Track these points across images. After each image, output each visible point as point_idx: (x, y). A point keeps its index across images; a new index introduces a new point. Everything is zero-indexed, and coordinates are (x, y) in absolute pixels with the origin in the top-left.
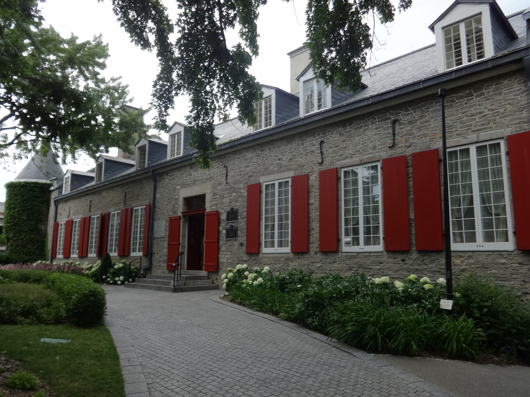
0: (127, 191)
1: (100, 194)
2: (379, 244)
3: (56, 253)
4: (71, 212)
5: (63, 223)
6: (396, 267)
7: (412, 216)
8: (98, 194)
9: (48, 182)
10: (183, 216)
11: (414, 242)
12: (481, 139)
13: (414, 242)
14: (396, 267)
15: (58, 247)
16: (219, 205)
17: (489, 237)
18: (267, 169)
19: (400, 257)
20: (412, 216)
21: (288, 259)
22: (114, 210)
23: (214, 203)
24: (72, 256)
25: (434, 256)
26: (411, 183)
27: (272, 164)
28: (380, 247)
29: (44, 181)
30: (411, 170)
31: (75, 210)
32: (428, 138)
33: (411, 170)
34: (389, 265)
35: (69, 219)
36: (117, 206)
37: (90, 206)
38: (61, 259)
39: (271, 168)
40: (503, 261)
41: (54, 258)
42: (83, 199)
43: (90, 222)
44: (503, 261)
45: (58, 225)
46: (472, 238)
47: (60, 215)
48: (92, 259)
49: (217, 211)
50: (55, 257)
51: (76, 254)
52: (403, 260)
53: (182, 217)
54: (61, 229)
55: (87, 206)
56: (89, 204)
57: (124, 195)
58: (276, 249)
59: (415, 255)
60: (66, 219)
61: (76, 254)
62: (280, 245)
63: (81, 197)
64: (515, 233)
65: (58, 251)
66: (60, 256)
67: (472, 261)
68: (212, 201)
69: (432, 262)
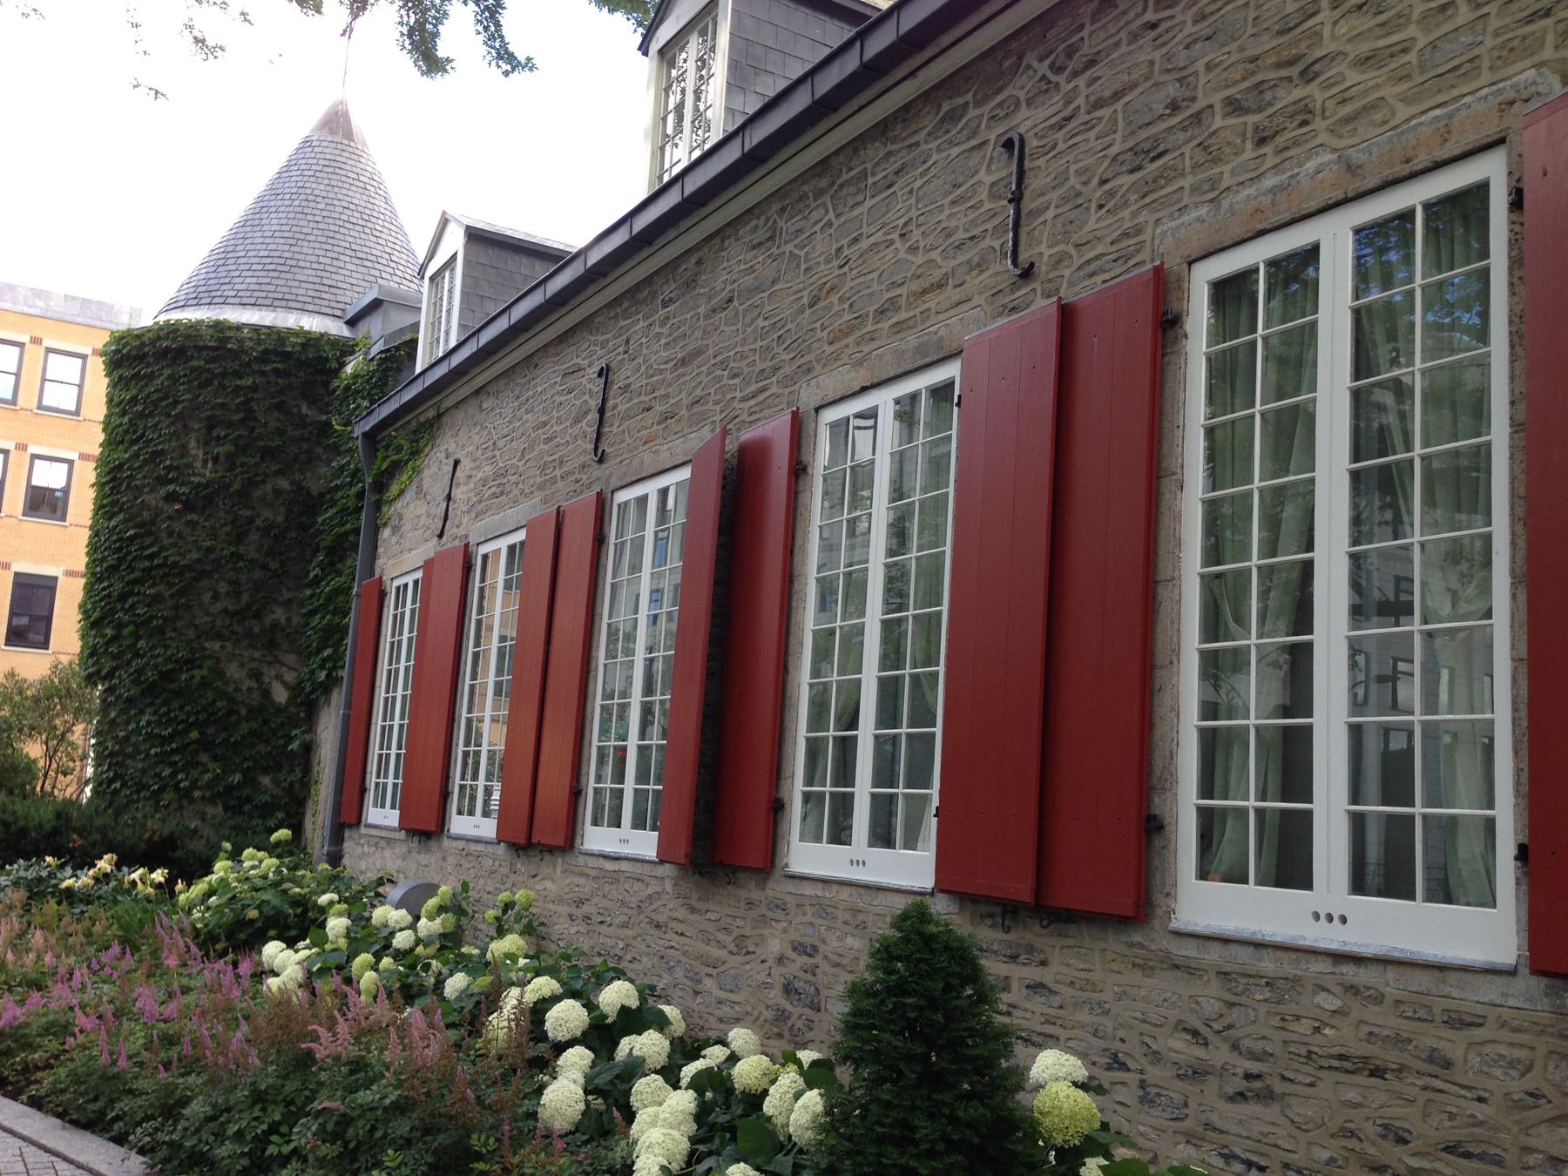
0: (1026, 121)
1: (691, 284)
3: (363, 790)
4: (458, 493)
5: (410, 579)
8: (667, 291)
9: (337, 329)
15: (375, 751)
22: (862, 377)
24: (460, 824)
29: (312, 324)
31: (488, 470)
35: (451, 542)
36: (899, 327)
37: (602, 411)
38: (383, 839)
41: (350, 826)
42: (547, 381)
43: (600, 540)
45: (382, 595)
47: (395, 529)
48: (615, 878)
50: (357, 821)
51: (486, 814)
54: (398, 620)
55: (577, 420)
56: (594, 403)
57: (994, 171)
60: (428, 550)
61: (486, 814)
63: (529, 362)
65: (372, 780)
66: (381, 815)
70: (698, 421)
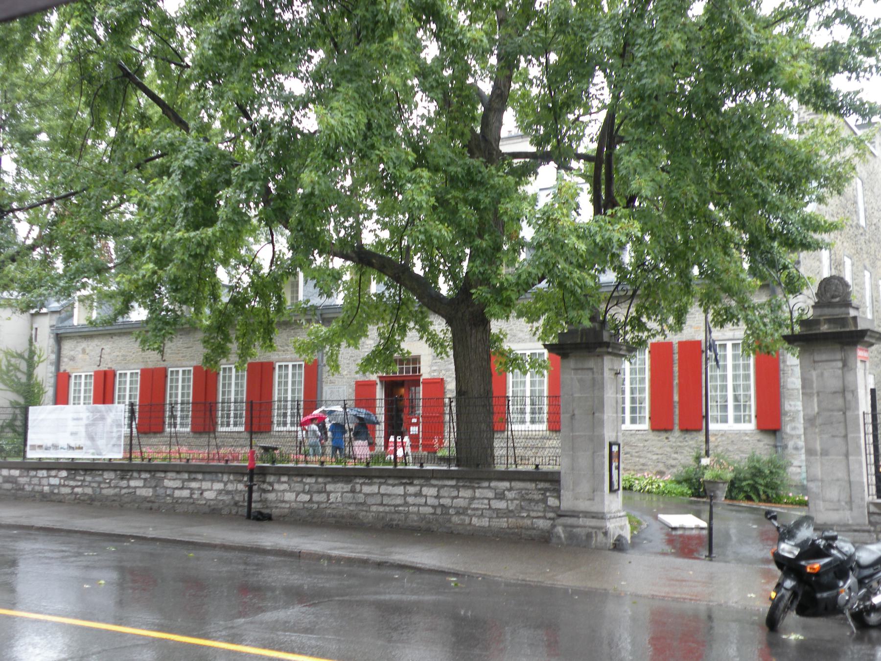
2: (645, 423)
6: (660, 444)
7: (676, 398)
10: (381, 381)
11: (676, 420)
12: (736, 337)
13: (676, 420)
14: (660, 444)
16: (443, 372)
17: (737, 420)
18: (514, 336)
19: (664, 435)
20: (676, 398)
21: (543, 438)
23: (435, 368)
25: (695, 434)
26: (676, 369)
27: (522, 331)
28: (646, 426)
30: (676, 357)
32: (693, 330)
33: (676, 357)
34: (654, 443)
39: (521, 335)
40: (747, 438)
44: (747, 438)
46: (725, 420)
49: (442, 379)
52: (667, 438)
53: (378, 381)
58: (528, 426)
59: (677, 433)
62: (533, 421)
64: (756, 416)
67: (724, 438)
68: (431, 366)
69: (692, 439)
70: (193, 360)
